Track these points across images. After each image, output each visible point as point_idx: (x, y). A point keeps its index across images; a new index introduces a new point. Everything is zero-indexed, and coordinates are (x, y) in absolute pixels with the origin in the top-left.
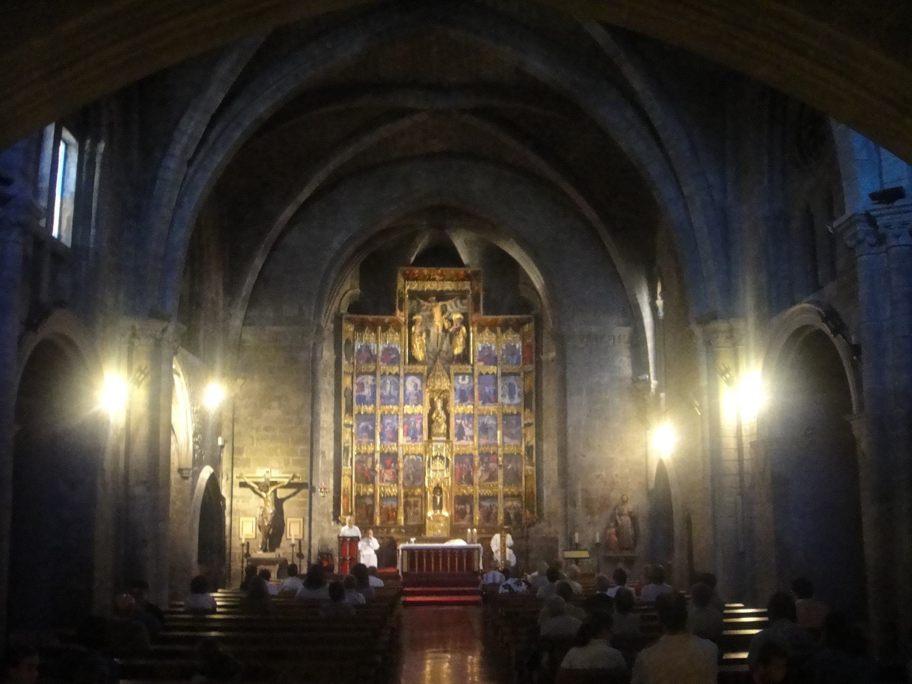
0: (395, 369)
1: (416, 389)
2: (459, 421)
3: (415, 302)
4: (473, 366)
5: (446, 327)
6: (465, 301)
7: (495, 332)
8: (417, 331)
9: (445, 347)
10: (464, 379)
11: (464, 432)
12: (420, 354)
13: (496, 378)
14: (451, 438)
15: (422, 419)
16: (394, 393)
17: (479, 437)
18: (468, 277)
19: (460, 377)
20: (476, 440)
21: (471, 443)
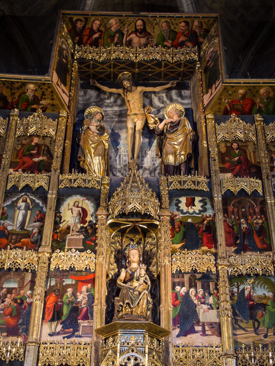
0: (40, 180)
1: (83, 221)
2: (183, 290)
3: (92, 93)
4: (209, 177)
5: (152, 126)
6: (185, 93)
7: (253, 122)
8: (93, 128)
9: (147, 162)
10: (191, 203)
11: (195, 314)
12: (96, 164)
13: (264, 202)
14: (163, 325)
15: (93, 281)
16: (32, 227)
17: (235, 325)
18: (194, 39)
19: (183, 200)
20: (226, 331)
21: (215, 340)
